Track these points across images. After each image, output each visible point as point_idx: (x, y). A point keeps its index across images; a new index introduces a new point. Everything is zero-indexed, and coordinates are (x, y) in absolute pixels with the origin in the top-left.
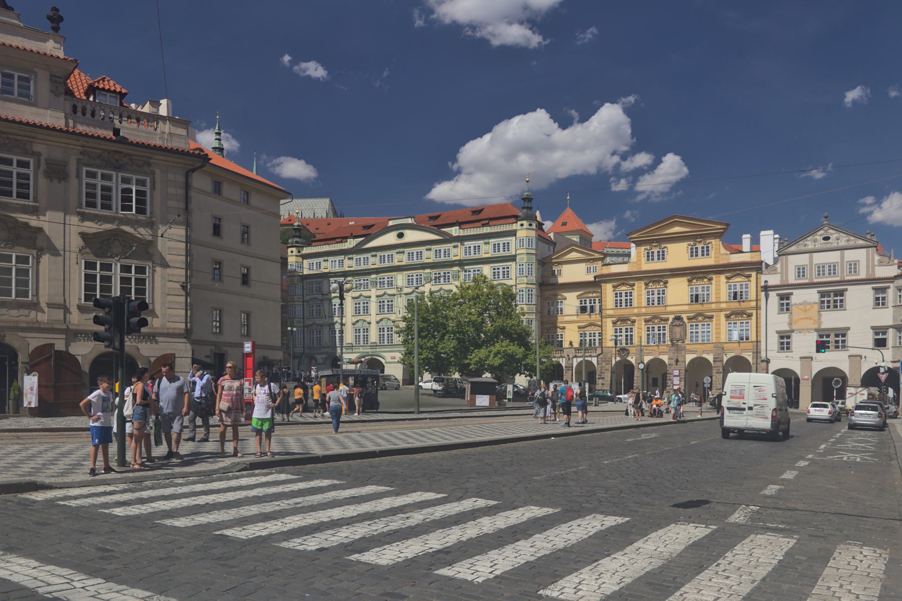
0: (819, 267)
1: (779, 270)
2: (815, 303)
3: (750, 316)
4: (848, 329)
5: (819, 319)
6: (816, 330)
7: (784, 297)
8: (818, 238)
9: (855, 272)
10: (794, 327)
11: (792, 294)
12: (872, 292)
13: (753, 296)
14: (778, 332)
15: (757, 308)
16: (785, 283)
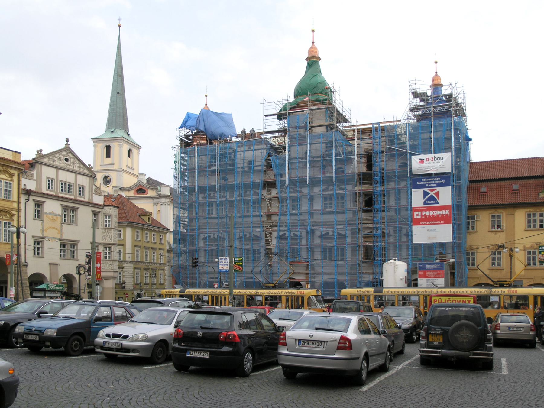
0: (62, 184)
1: (35, 178)
2: (59, 215)
3: (12, 216)
4: (78, 241)
5: (61, 230)
6: (60, 240)
7: (39, 204)
8: (62, 157)
9: (83, 195)
10: (46, 234)
11: (44, 202)
12: (91, 214)
13: (15, 197)
14: (33, 237)
15: (19, 211)
16: (38, 191)
